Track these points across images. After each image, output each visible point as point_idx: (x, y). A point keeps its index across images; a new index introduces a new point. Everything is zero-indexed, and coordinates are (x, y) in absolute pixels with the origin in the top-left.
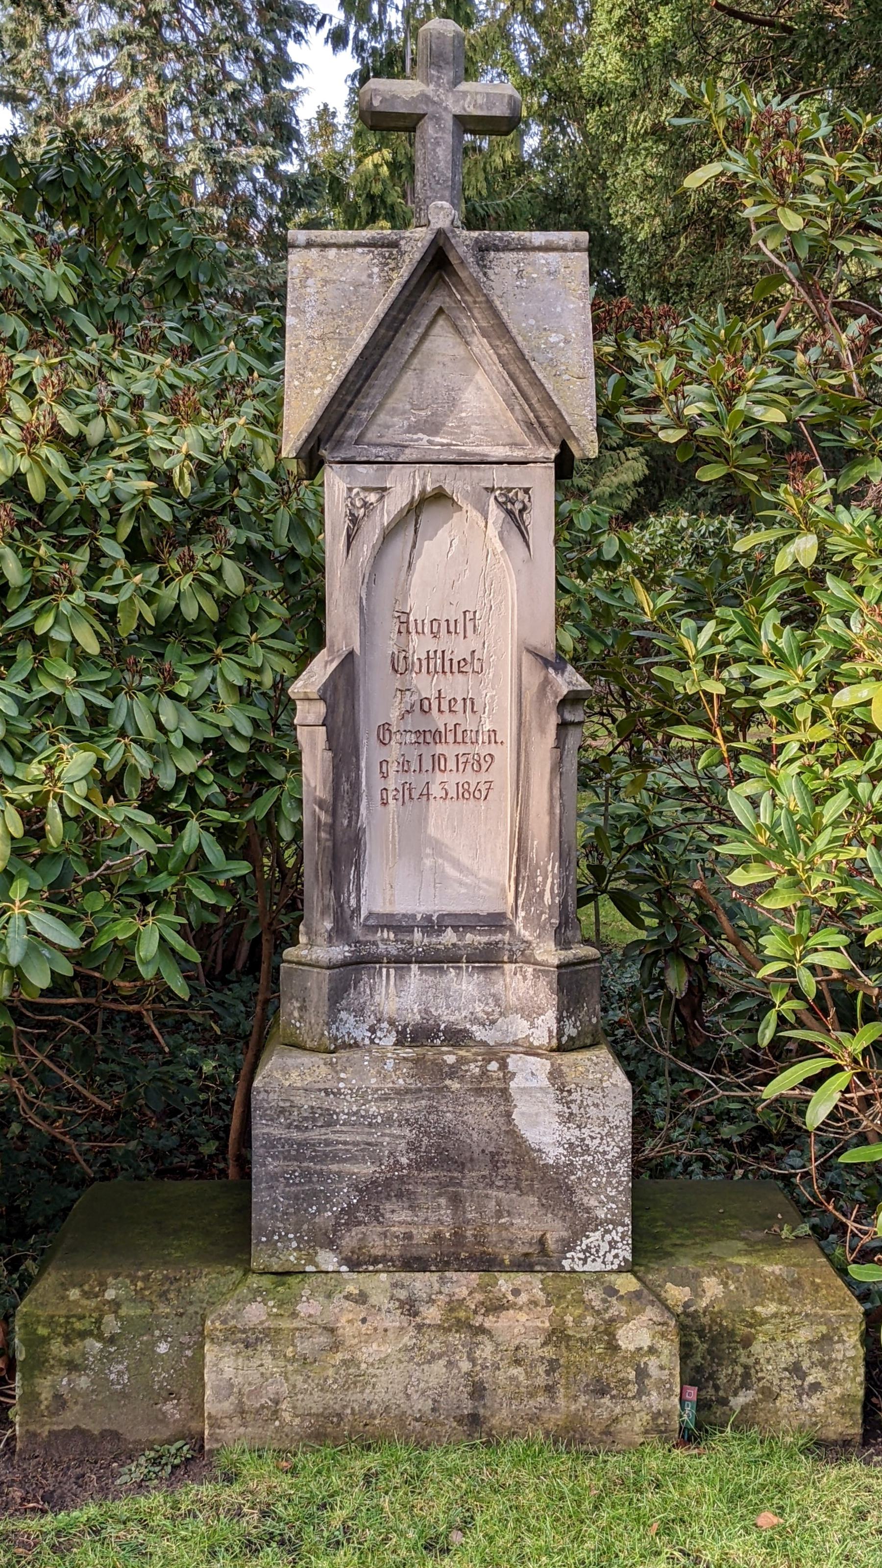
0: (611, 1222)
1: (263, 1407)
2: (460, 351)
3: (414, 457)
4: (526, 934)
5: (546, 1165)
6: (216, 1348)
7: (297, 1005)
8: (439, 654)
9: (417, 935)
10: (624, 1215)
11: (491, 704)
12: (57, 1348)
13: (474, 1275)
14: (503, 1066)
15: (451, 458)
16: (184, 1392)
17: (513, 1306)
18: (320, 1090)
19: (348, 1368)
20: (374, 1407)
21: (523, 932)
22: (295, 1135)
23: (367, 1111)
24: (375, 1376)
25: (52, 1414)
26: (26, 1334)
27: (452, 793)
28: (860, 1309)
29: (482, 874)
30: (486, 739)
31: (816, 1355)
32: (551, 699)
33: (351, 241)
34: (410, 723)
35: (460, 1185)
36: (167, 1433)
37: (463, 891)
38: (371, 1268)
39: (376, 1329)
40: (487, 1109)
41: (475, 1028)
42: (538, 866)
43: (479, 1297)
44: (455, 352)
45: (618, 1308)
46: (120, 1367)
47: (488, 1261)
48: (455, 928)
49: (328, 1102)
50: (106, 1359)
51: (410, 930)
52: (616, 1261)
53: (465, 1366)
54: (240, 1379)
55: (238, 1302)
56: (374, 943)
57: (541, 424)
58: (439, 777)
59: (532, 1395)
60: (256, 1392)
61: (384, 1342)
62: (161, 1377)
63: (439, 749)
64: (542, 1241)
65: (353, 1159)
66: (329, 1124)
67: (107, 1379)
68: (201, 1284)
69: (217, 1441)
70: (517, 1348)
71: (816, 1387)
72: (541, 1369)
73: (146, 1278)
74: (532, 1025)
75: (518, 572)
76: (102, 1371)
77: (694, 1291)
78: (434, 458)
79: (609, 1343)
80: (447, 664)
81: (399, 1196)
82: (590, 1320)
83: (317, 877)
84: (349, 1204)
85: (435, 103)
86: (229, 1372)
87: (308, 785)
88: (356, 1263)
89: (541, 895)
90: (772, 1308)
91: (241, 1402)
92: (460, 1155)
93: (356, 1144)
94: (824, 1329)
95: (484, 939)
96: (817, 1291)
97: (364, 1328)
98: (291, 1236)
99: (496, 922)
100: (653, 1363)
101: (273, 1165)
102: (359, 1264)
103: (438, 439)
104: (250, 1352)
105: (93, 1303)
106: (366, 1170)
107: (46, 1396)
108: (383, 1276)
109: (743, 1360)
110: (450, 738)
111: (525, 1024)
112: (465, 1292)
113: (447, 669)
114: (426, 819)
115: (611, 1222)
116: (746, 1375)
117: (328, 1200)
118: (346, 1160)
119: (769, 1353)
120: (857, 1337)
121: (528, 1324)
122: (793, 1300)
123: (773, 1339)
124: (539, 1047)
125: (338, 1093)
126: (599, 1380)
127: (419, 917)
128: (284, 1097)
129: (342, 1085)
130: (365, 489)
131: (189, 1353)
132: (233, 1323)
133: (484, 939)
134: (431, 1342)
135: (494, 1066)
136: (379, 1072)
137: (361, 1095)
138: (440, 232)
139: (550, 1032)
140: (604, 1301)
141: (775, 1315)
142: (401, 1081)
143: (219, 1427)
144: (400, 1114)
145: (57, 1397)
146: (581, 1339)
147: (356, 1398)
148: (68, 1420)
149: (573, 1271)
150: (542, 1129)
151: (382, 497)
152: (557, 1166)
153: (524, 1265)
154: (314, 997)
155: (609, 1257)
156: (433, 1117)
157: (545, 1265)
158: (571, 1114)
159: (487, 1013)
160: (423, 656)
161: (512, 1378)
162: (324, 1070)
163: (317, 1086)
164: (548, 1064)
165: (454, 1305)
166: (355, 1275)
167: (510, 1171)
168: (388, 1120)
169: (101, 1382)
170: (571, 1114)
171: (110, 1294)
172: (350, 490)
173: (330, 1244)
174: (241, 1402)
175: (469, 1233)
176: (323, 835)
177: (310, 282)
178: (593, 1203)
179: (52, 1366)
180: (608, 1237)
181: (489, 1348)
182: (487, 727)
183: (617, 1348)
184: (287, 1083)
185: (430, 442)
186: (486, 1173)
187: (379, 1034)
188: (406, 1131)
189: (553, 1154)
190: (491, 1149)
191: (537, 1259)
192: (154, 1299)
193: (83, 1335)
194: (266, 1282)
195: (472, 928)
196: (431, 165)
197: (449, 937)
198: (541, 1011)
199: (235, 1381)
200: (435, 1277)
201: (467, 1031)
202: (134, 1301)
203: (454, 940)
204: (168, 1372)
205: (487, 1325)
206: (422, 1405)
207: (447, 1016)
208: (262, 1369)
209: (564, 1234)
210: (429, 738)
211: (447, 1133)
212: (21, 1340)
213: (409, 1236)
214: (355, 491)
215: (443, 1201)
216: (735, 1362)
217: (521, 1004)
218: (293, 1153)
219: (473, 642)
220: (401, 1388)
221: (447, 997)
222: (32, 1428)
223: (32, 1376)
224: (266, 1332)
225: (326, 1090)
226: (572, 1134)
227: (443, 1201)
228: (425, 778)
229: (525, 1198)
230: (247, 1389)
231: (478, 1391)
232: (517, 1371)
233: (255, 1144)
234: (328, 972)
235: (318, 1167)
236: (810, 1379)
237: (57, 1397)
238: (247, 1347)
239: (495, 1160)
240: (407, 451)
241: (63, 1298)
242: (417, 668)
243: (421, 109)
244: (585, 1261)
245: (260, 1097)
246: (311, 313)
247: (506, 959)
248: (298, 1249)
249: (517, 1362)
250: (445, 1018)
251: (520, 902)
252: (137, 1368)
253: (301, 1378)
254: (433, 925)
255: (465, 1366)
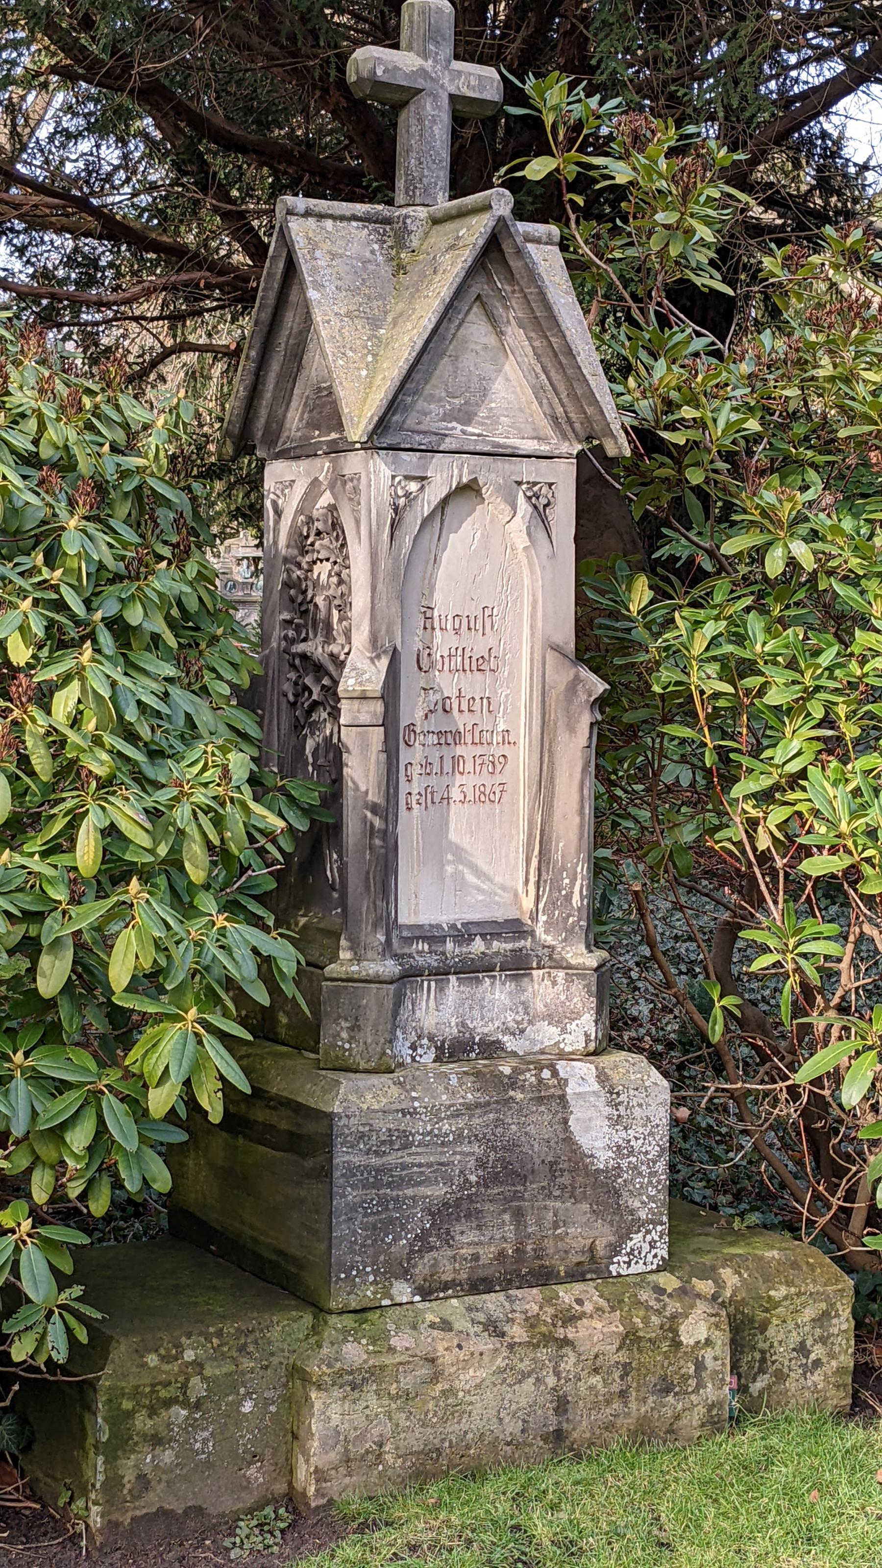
0: (652, 1222)
1: (367, 1452)
2: (492, 340)
3: (454, 447)
4: (549, 939)
5: (598, 1170)
6: (323, 1395)
7: (345, 1024)
8: (460, 652)
9: (449, 945)
10: (662, 1214)
11: (505, 703)
12: (142, 1422)
13: (535, 1291)
14: (555, 1073)
15: (487, 448)
16: (268, 1452)
17: (583, 1315)
18: (397, 1111)
19: (447, 1398)
20: (470, 1436)
21: (543, 936)
22: (374, 1161)
23: (440, 1129)
24: (471, 1403)
25: (135, 1498)
26: (109, 1410)
27: (470, 797)
28: (849, 1282)
29: (498, 879)
30: (500, 739)
31: (818, 1332)
32: (583, 697)
33: (348, 214)
34: (433, 724)
35: (522, 1198)
36: (249, 1500)
37: (480, 898)
38: (441, 1295)
39: (472, 1354)
40: (548, 1117)
41: (506, 1038)
42: (564, 868)
43: (550, 1311)
44: (484, 340)
45: (673, 1306)
46: (206, 1434)
47: (547, 1274)
48: (483, 936)
49: (406, 1123)
50: (191, 1426)
51: (442, 940)
52: (656, 1261)
53: (551, 1381)
54: (346, 1426)
55: (332, 1344)
56: (410, 956)
57: (569, 419)
58: (459, 779)
59: (608, 1403)
60: (361, 1438)
61: (480, 1366)
62: (245, 1438)
63: (459, 750)
64: (592, 1249)
65: (427, 1182)
66: (406, 1146)
67: (192, 1450)
68: (275, 1333)
69: (323, 1496)
70: (596, 1356)
71: (817, 1363)
72: (617, 1374)
73: (219, 1333)
74: (564, 1031)
75: (543, 568)
76: (187, 1442)
77: (715, 1282)
78: (471, 448)
79: (673, 1340)
80: (467, 661)
81: (468, 1216)
82: (655, 1320)
83: (368, 888)
84: (422, 1230)
85: (432, 78)
86: (336, 1419)
87: (357, 788)
88: (427, 1291)
89: (569, 897)
90: (783, 1291)
91: (347, 1450)
92: (522, 1167)
93: (429, 1165)
94: (823, 1306)
95: (509, 946)
96: (813, 1271)
97: (462, 1355)
98: (368, 1269)
99: (515, 928)
100: (708, 1354)
101: (352, 1195)
102: (431, 1293)
103: (470, 429)
104: (356, 1394)
105: (175, 1367)
106: (438, 1191)
107: (129, 1477)
108: (454, 1302)
109: (761, 1345)
110: (469, 740)
111: (554, 1030)
112: (536, 1308)
113: (467, 667)
114: (447, 824)
115: (652, 1222)
116: (763, 1360)
117: (403, 1227)
118: (420, 1184)
119: (781, 1336)
120: (849, 1310)
121: (605, 1330)
122: (797, 1281)
123: (784, 1321)
124: (572, 1053)
125: (413, 1113)
126: (664, 1378)
127: (445, 926)
128: (364, 1121)
129: (416, 1104)
130: (407, 478)
131: (273, 1409)
132: (338, 1365)
133: (509, 946)
134: (522, 1360)
135: (546, 1074)
136: (446, 1088)
137: (435, 1114)
138: (501, 220)
139: (587, 1035)
140: (658, 1300)
141: (786, 1298)
142: (469, 1095)
143: (325, 1481)
144: (470, 1130)
145: (142, 1478)
146: (650, 1340)
147: (453, 1428)
148: (150, 1503)
149: (619, 1276)
150: (595, 1135)
151: (422, 488)
152: (606, 1171)
153: (577, 1275)
154: (373, 1015)
155: (650, 1257)
156: (500, 1130)
157: (595, 1272)
158: (619, 1116)
159: (517, 1023)
160: (446, 654)
161: (591, 1388)
162: (395, 1091)
163: (394, 1107)
164: (592, 1067)
165: (532, 1322)
166: (427, 1304)
167: (566, 1180)
168: (459, 1137)
169: (187, 1452)
170: (619, 1116)
171: (189, 1355)
172: (393, 477)
173: (405, 1274)
174: (347, 1450)
175: (529, 1248)
176: (377, 842)
177: (318, 254)
178: (637, 1204)
179: (136, 1444)
180: (649, 1238)
181: (572, 1359)
182: (502, 727)
183: (679, 1344)
184: (365, 1107)
185: (464, 432)
186: (545, 1184)
187: (419, 1051)
188: (476, 1148)
189: (603, 1158)
190: (550, 1159)
191: (590, 1268)
192: (235, 1355)
193: (168, 1403)
194: (348, 1321)
195: (497, 936)
196: (429, 143)
197: (478, 946)
198: (575, 1015)
199: (341, 1428)
200: (501, 1296)
201: (498, 1042)
202: (215, 1359)
203: (482, 949)
204: (252, 1432)
205: (570, 1336)
206: (513, 1427)
207: (483, 1027)
208: (367, 1412)
209: (612, 1239)
210: (450, 740)
211: (511, 1146)
212: (104, 1419)
213: (476, 1257)
214: (397, 479)
215: (507, 1217)
216: (754, 1348)
217: (551, 1013)
218: (371, 1180)
219: (491, 641)
220: (495, 1413)
221: (483, 1007)
222: (114, 1517)
223: (116, 1458)
224: (371, 1371)
225: (403, 1111)
226: (619, 1137)
227: (507, 1217)
228: (446, 780)
229: (578, 1206)
230: (353, 1434)
231: (562, 1405)
232: (596, 1380)
233: (337, 1174)
234: (392, 987)
235: (395, 1193)
236: (813, 1356)
237: (142, 1478)
238: (353, 1389)
239: (553, 1168)
240: (447, 440)
241: (144, 1365)
242: (439, 667)
243: (420, 83)
244: (629, 1264)
245: (341, 1124)
246: (330, 288)
247: (534, 965)
248: (375, 1283)
249: (596, 1371)
250: (479, 1030)
251: (541, 906)
252: (222, 1433)
253: (403, 1416)
254: (464, 933)
255: (551, 1381)
